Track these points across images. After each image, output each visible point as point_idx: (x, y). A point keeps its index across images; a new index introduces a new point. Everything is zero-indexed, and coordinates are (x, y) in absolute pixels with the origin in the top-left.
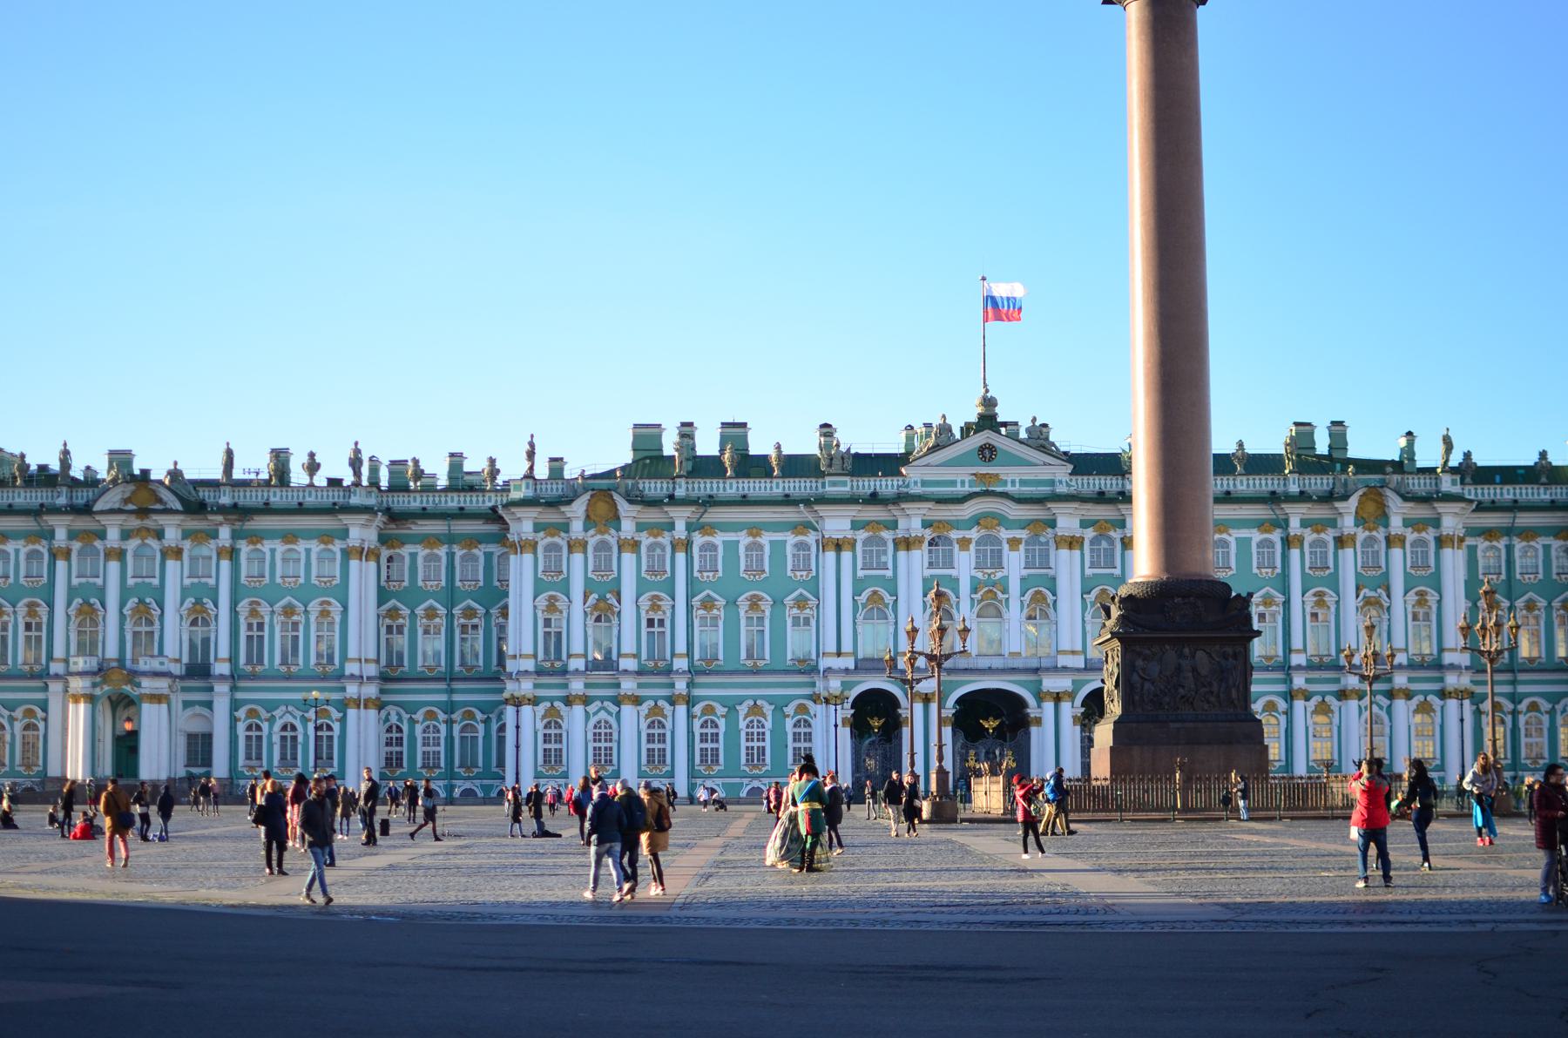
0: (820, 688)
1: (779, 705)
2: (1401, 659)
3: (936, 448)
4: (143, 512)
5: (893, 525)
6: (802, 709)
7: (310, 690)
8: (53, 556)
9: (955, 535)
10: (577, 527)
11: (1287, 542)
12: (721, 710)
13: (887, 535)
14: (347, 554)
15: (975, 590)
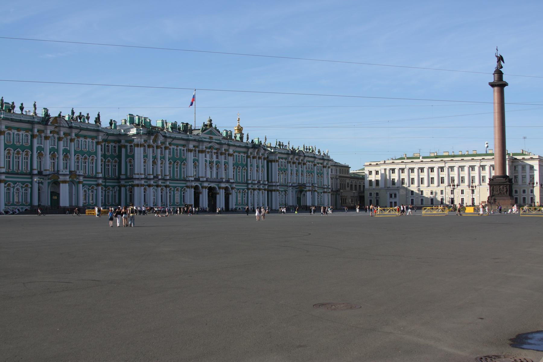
0: (189, 184)
1: (182, 187)
2: (261, 182)
3: (205, 130)
4: (56, 127)
5: (198, 147)
6: (185, 189)
7: (129, 182)
8: (33, 136)
9: (207, 150)
10: (151, 141)
11: (248, 157)
12: (173, 189)
13: (197, 149)
14: (98, 143)
15: (210, 163)
